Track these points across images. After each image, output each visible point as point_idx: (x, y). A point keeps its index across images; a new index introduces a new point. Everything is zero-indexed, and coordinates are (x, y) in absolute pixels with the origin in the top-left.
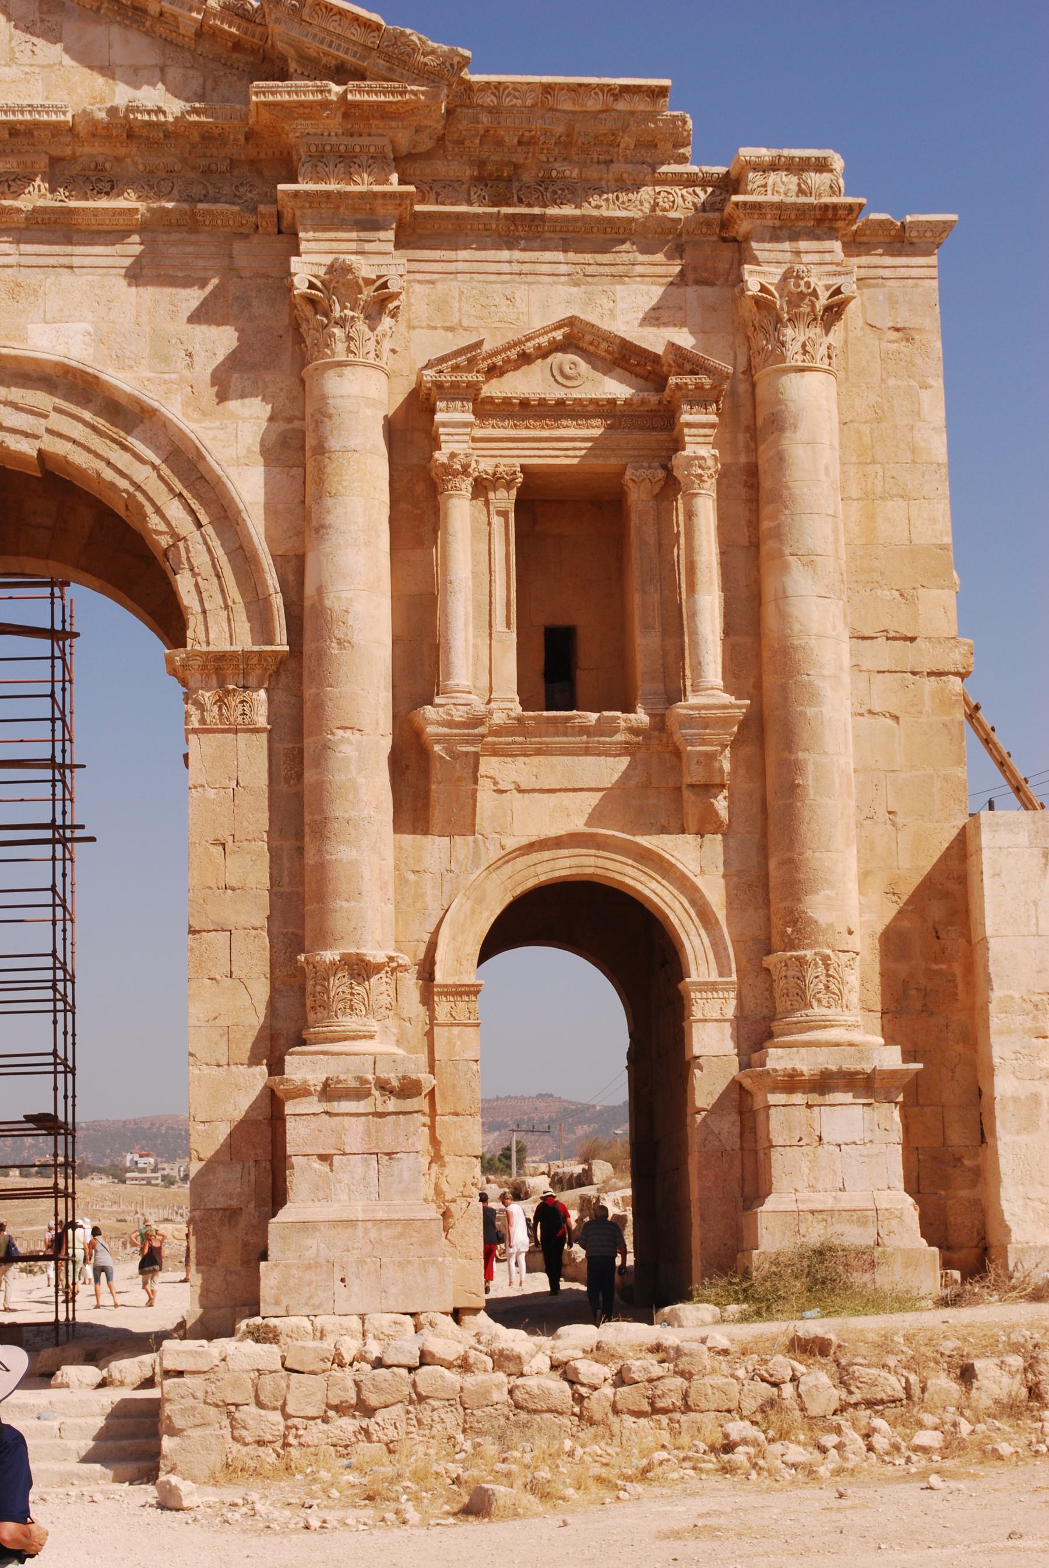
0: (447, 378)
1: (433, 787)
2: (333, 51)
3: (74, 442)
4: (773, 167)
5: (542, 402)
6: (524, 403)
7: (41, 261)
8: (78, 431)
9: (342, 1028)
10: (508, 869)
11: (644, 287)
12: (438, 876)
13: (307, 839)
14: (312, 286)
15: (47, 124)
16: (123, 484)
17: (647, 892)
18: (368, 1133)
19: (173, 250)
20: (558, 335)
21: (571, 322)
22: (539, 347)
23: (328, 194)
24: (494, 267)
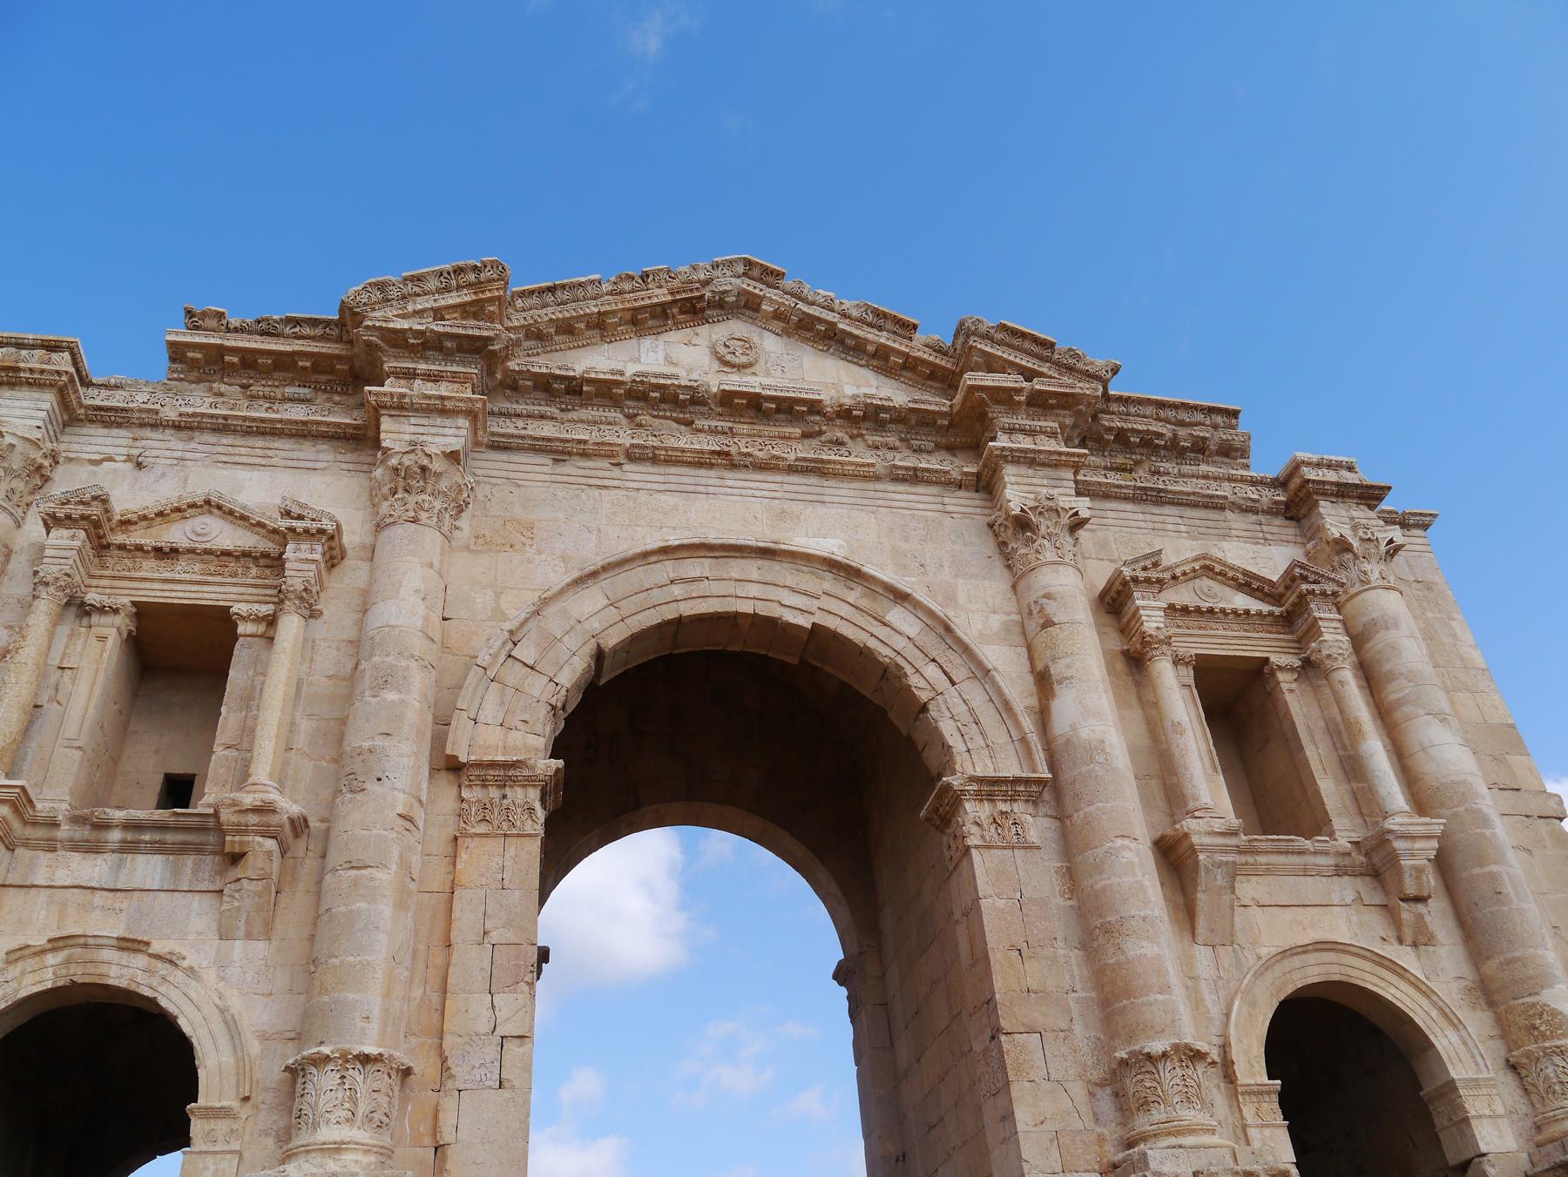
0: (1142, 575)
1: (1199, 895)
2: (1018, 360)
3: (842, 618)
5: (1198, 610)
6: (1185, 610)
8: (845, 610)
9: (1187, 1122)
10: (1269, 976)
11: (1242, 545)
12: (1211, 982)
14: (1022, 510)
16: (885, 651)
17: (1389, 997)
21: (1204, 557)
22: (1184, 574)
24: (1134, 524)
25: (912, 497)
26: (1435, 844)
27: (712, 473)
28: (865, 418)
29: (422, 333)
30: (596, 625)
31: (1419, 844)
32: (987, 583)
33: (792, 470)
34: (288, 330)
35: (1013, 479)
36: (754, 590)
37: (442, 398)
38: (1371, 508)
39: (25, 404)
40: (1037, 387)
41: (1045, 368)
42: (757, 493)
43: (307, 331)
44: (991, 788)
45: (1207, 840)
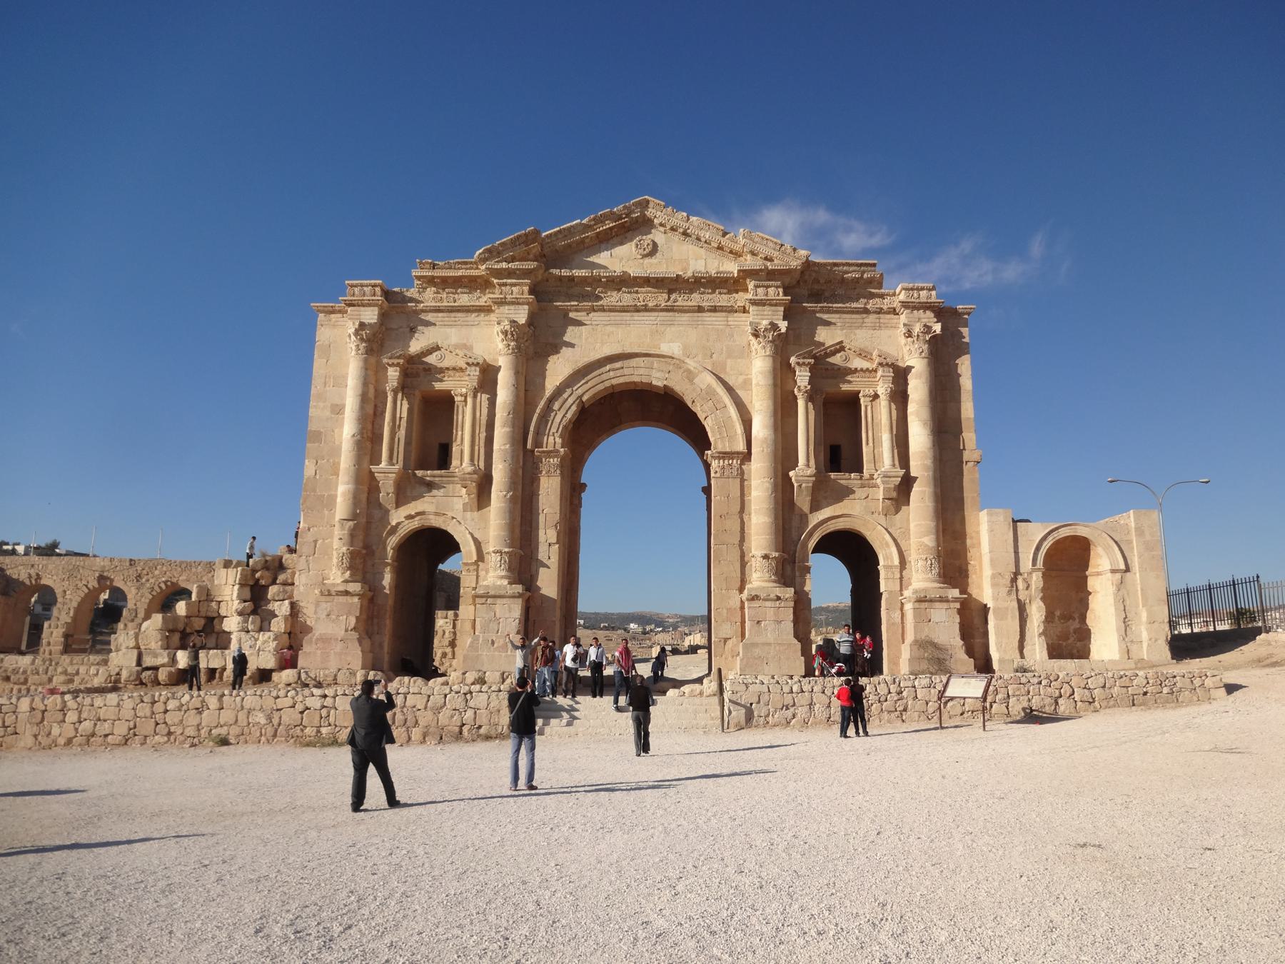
0: (801, 361)
4: (912, 289)
7: (665, 323)
13: (753, 515)
15: (668, 278)
18: (775, 614)
19: (708, 319)
20: (838, 347)
21: (842, 342)
22: (831, 351)
23: (762, 300)
25: (714, 319)
26: (900, 479)
27: (628, 314)
28: (695, 282)
29: (505, 269)
30: (580, 391)
31: (894, 479)
32: (739, 360)
33: (662, 310)
34: (457, 267)
35: (755, 313)
36: (642, 371)
37: (517, 298)
38: (933, 312)
39: (369, 313)
40: (770, 267)
41: (776, 254)
42: (647, 322)
43: (463, 266)
44: (724, 455)
45: (801, 478)
